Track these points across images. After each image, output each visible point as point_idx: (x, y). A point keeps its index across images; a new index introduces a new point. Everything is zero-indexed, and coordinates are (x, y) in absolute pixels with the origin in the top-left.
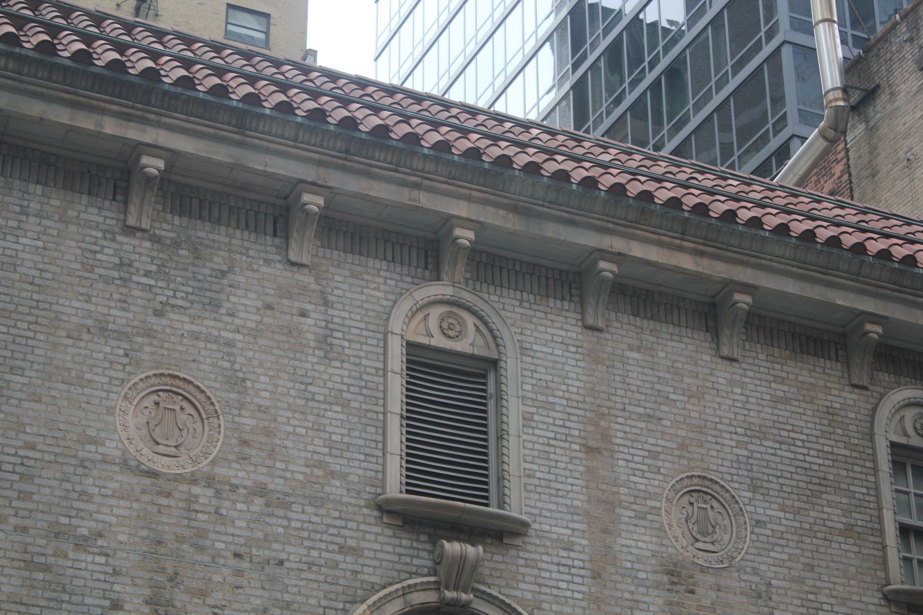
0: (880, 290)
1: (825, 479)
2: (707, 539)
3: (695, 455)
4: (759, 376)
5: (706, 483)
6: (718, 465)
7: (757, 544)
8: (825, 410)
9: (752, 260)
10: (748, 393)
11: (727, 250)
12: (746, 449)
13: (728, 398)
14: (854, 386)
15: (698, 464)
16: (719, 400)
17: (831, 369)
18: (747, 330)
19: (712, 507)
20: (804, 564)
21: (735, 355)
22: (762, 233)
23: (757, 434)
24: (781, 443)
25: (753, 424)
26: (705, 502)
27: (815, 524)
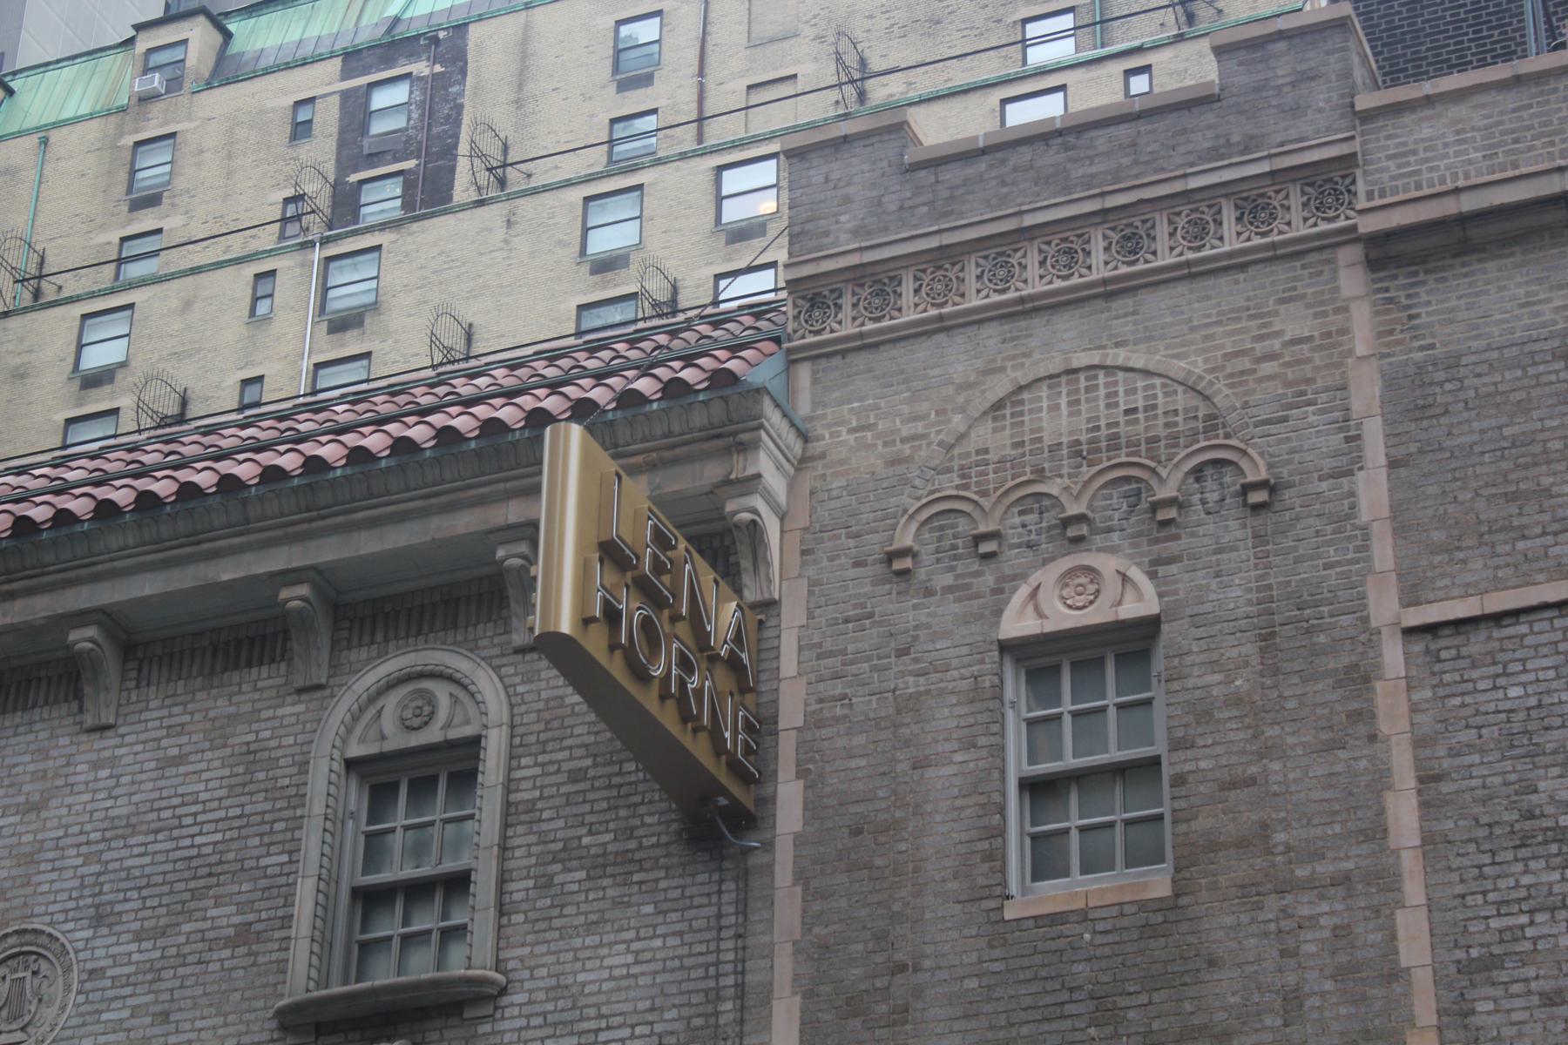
0: (290, 530)
1: (221, 862)
2: (14, 1026)
3: (16, 902)
4: (143, 737)
5: (29, 937)
6: (47, 904)
7: (83, 1009)
8: (244, 749)
9: (83, 572)
10: (120, 771)
11: (43, 574)
12: (99, 861)
13: (86, 791)
14: (301, 691)
15: (18, 913)
16: (69, 800)
17: (269, 677)
18: (140, 670)
19: (35, 973)
20: (154, 1015)
21: (103, 721)
22: (78, 528)
23: (120, 832)
24: (156, 832)
25: (119, 817)
26: (26, 968)
27: (187, 942)
